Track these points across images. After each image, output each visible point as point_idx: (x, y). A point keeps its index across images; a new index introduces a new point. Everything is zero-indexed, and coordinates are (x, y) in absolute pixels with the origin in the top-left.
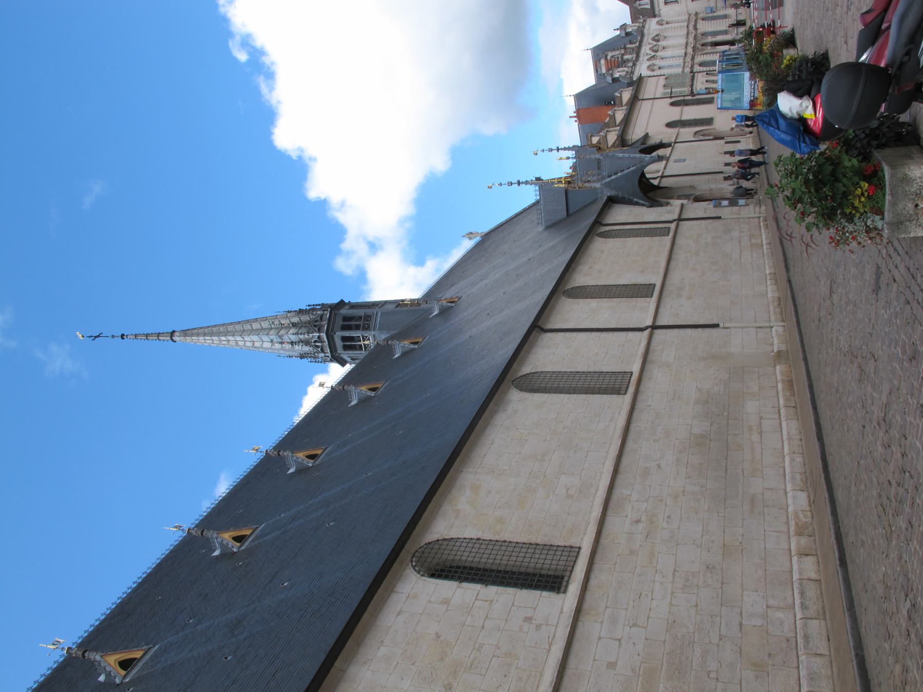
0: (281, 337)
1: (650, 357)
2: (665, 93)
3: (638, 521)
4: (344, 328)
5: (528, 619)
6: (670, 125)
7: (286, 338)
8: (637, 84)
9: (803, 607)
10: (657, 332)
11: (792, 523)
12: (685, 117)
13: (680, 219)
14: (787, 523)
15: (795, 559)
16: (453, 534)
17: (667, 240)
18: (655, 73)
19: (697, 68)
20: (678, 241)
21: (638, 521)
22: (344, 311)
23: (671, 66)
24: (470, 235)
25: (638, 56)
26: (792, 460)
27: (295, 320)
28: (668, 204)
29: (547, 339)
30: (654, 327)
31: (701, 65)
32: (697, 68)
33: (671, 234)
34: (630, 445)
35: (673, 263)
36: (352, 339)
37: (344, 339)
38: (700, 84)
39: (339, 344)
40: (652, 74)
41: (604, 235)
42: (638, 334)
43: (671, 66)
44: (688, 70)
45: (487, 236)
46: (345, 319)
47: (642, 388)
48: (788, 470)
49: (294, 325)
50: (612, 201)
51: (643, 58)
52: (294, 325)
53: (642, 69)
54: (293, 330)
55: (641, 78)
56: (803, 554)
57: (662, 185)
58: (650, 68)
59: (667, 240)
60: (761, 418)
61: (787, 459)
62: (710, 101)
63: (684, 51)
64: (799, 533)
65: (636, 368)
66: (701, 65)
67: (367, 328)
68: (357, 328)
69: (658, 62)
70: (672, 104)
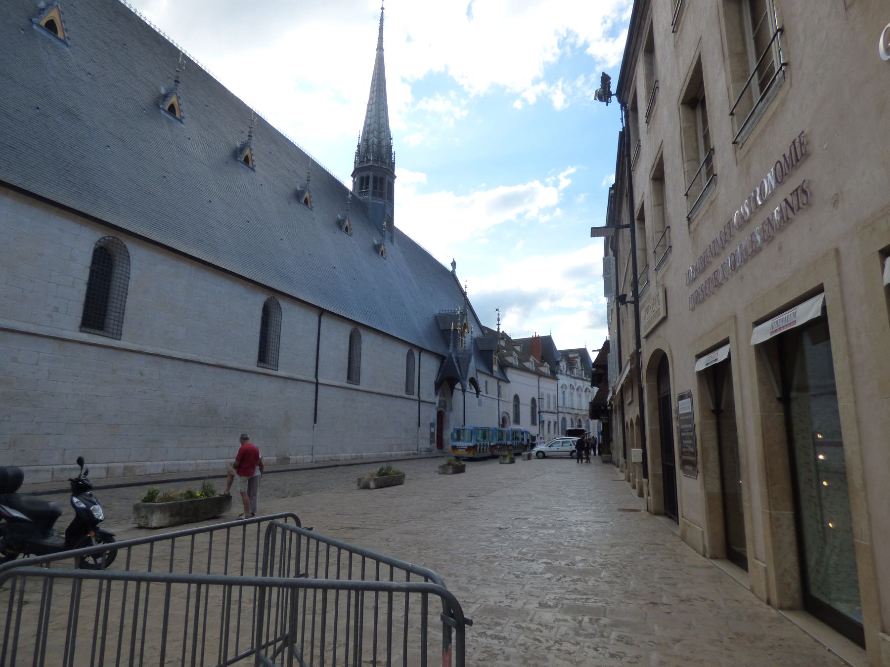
0: (373, 132)
1: (289, 381)
2: (543, 395)
3: (141, 374)
4: (375, 179)
5: (56, 310)
6: (516, 398)
7: (371, 135)
8: (553, 375)
9: (62, 470)
10: (314, 386)
11: (135, 464)
12: (522, 408)
13: (420, 401)
14: (137, 461)
15: (105, 465)
16: (134, 262)
17: (404, 394)
18: (560, 389)
19: (561, 416)
20: (399, 400)
21: (141, 374)
22: (387, 178)
23: (564, 398)
24: (454, 264)
25: (575, 378)
26: (191, 465)
27: (384, 143)
28: (436, 394)
29: (313, 317)
30: (317, 384)
31: (564, 419)
32: (561, 416)
33: (406, 396)
34: (211, 369)
35: (378, 397)
36: (367, 183)
37: (368, 178)
38: (546, 417)
39: (365, 174)
40: (560, 386)
41: (410, 355)
42: (314, 374)
43: (564, 398)
44: (560, 410)
45: (452, 276)
46: (382, 180)
47: (261, 376)
48: (181, 462)
49: (380, 142)
50: (441, 358)
51: (572, 381)
52: (380, 142)
53: (563, 380)
54: (376, 140)
55: (557, 379)
56: (108, 470)
57: (455, 391)
58: (564, 386)
59: (404, 394)
60: (230, 447)
61: (193, 462)
62: (533, 423)
63: (576, 407)
64: (125, 468)
65: (280, 373)
66: (564, 419)
67: (374, 194)
68: (375, 188)
69: (568, 391)
70: (533, 400)
